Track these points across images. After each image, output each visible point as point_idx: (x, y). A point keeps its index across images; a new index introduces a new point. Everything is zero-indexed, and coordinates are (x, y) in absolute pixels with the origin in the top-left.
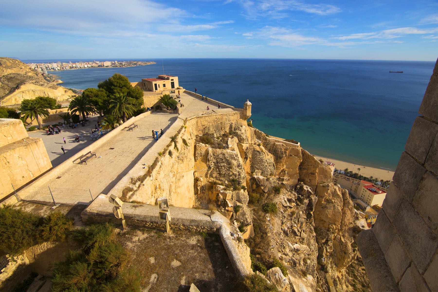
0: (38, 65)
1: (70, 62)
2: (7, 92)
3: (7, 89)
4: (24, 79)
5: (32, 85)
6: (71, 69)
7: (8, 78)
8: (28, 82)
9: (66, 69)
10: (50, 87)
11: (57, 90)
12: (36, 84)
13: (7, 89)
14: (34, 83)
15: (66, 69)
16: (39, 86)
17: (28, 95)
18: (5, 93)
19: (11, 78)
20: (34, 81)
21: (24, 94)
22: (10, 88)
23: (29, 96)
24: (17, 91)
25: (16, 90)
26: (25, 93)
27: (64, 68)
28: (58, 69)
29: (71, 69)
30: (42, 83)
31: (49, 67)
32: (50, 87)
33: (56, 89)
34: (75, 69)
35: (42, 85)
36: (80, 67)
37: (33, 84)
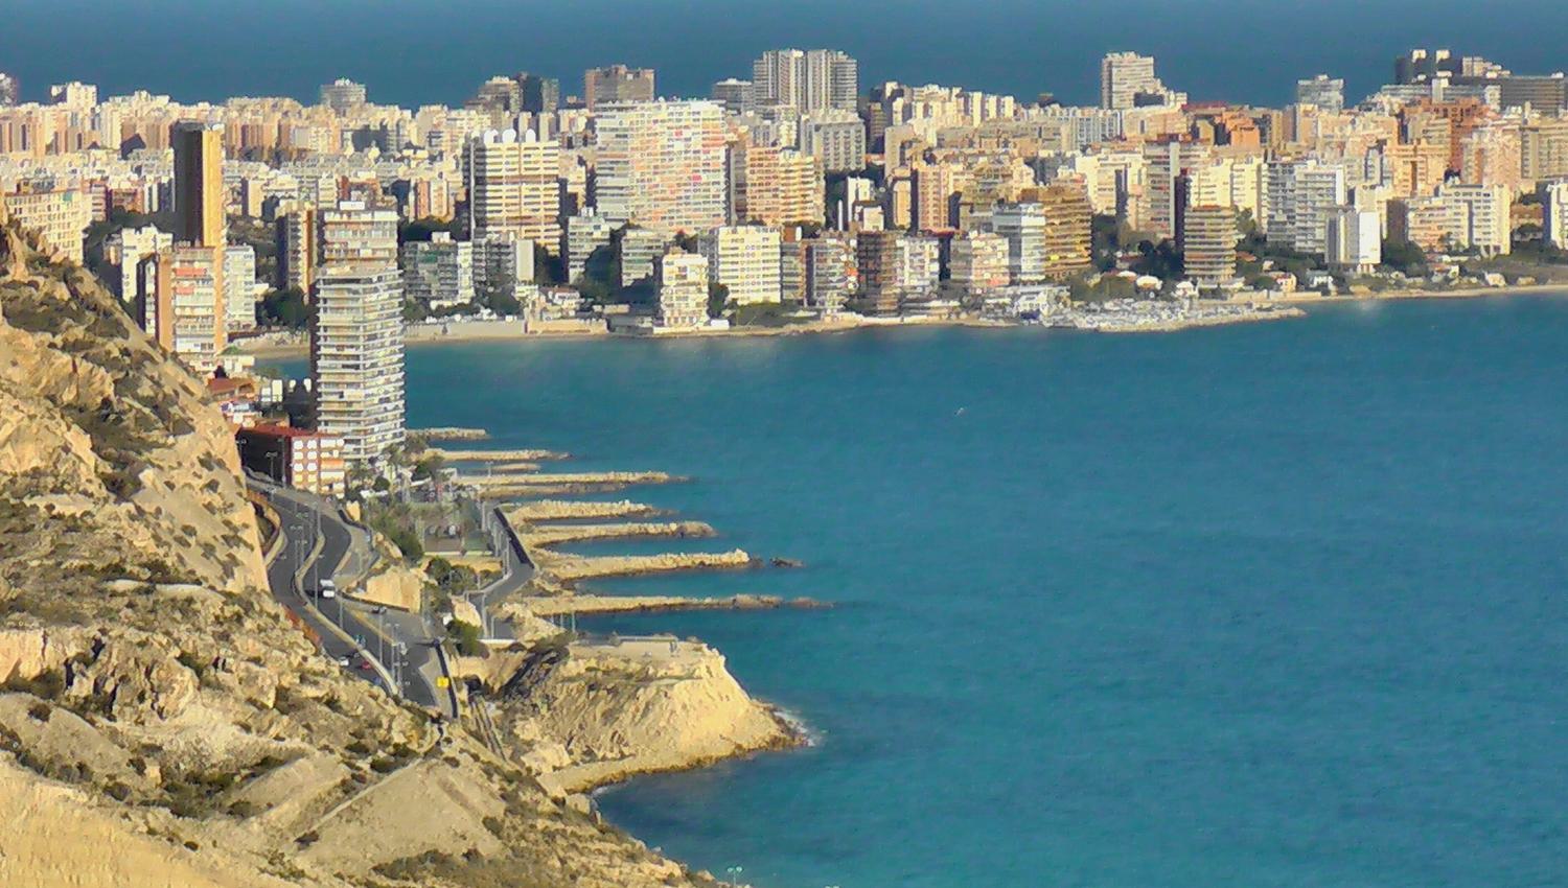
0: (212, 154)
6: (1114, 318)
15: (940, 312)
16: (111, 828)
27: (914, 265)
34: (1245, 304)
36: (1398, 253)
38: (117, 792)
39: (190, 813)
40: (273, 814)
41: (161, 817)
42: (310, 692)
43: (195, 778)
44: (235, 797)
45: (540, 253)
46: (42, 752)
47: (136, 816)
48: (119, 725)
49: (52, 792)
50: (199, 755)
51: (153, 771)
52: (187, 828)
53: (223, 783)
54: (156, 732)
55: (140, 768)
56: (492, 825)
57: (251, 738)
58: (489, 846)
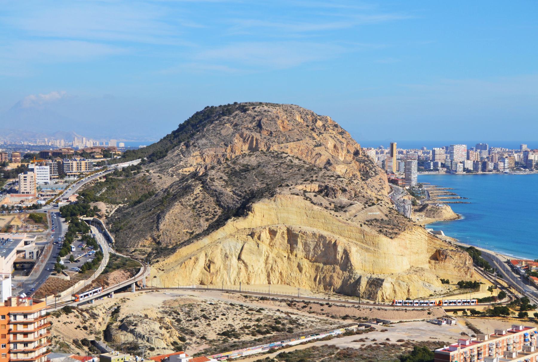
0: (395, 147)
1: (525, 147)
2: (205, 225)
3: (207, 213)
4: (284, 176)
5: (299, 201)
7: (237, 168)
8: (286, 191)
9: (494, 172)
10: (370, 222)
11: (395, 242)
12: (320, 198)
13: (207, 213)
14: (307, 195)
16: (325, 212)
17: (264, 247)
18: (192, 233)
19: (247, 169)
20: (315, 187)
21: (251, 243)
22: (219, 212)
23: (268, 257)
24: (231, 225)
25: (230, 222)
26: (256, 237)
27: (491, 166)
28: (465, 170)
29: (518, 173)
30: (343, 199)
31: (437, 157)
32: (370, 222)
33: (392, 236)
35: (340, 208)
37: (307, 198)
38: (326, 208)
39: (338, 211)
40: (350, 212)
41: (333, 212)
42: (360, 195)
43: (340, 207)
44: (345, 209)
45: (442, 164)
46: (315, 202)
47: (329, 211)
48: (329, 199)
49: (316, 207)
50: (341, 203)
51: (333, 205)
52: (336, 214)
53: (343, 207)
54: (335, 200)
55: (330, 204)
56: (387, 216)
57: (349, 201)
58: (385, 218)
